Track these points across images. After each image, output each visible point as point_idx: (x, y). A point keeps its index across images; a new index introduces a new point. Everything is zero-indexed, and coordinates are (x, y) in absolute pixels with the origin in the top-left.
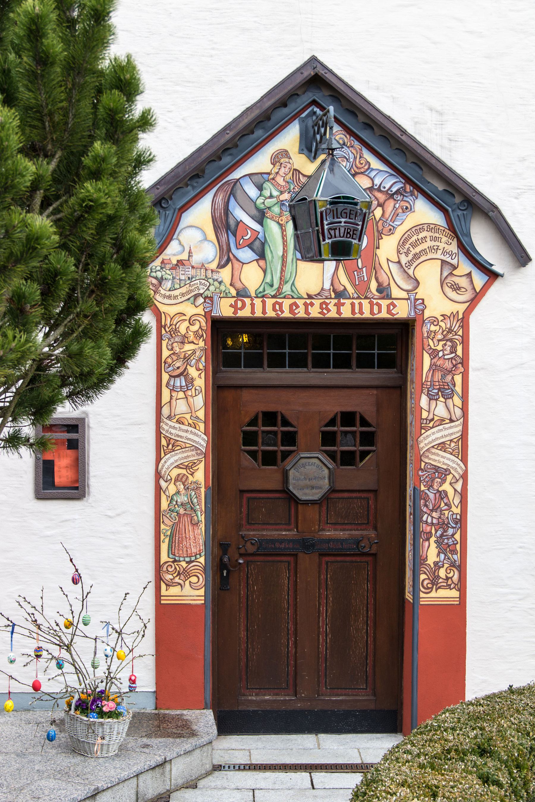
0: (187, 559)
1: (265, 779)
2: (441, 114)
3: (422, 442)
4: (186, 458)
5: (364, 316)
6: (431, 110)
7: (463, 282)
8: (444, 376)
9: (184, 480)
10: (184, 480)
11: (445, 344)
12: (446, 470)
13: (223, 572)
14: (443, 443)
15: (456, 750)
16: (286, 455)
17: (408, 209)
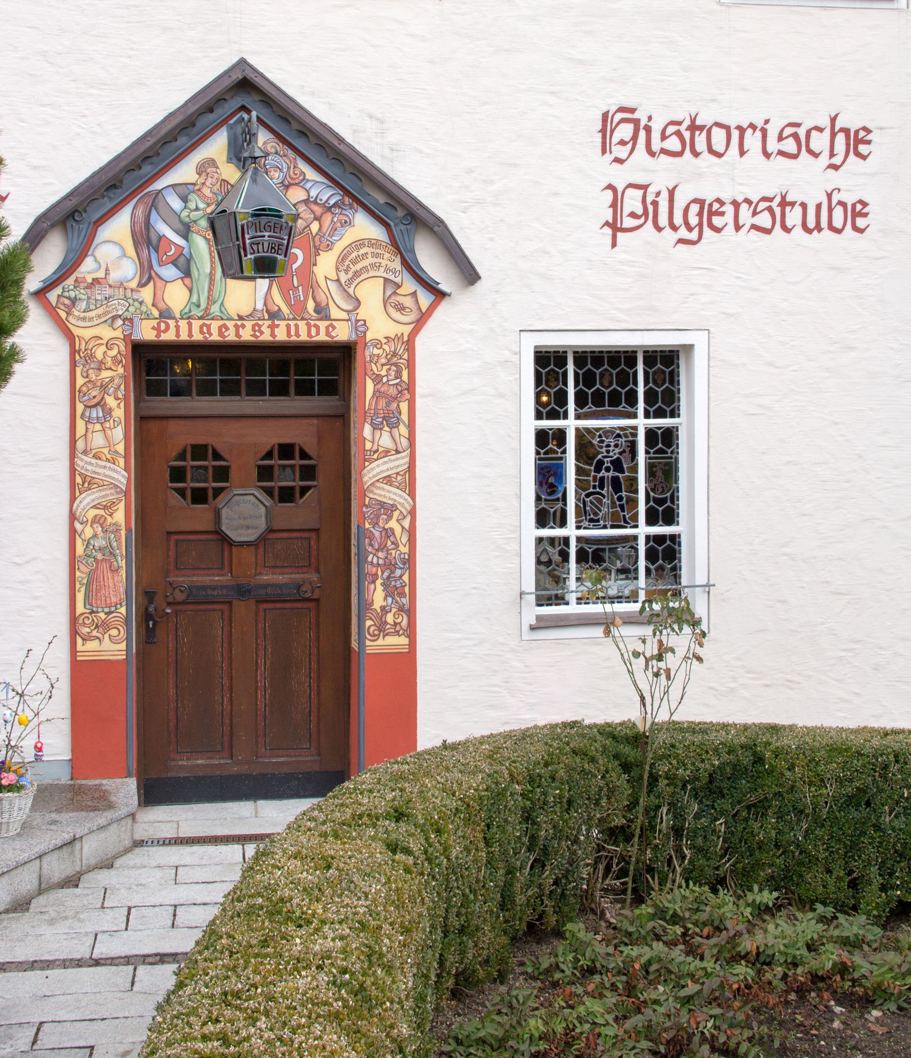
0: (107, 610)
1: (192, 853)
2: (382, 122)
3: (365, 475)
4: (103, 497)
5: (301, 339)
6: (371, 117)
7: (408, 302)
8: (388, 404)
9: (101, 521)
10: (101, 521)
11: (389, 369)
12: (392, 506)
13: (149, 623)
14: (389, 476)
15: (369, 815)
16: (218, 492)
17: (347, 223)
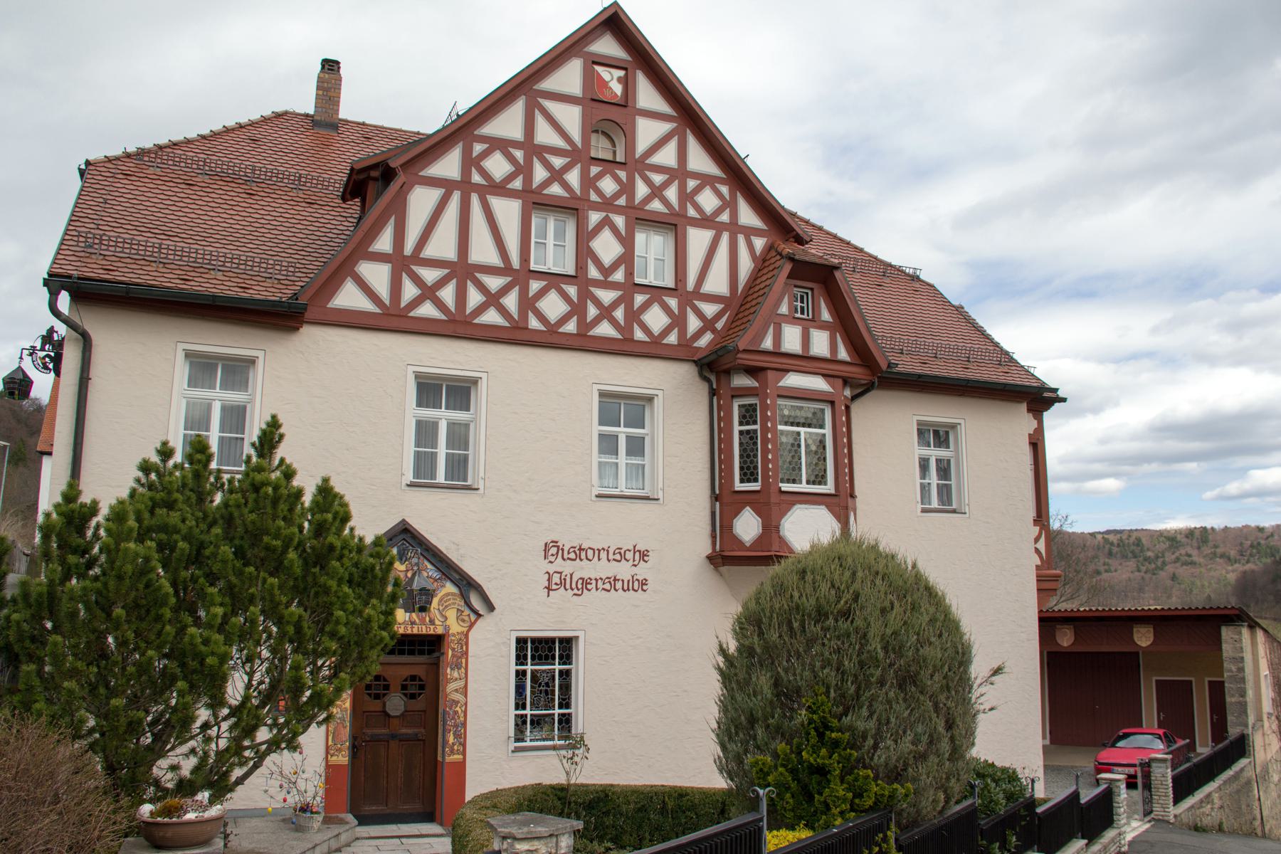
13: (355, 750)
16: (384, 695)
17: (443, 586)
